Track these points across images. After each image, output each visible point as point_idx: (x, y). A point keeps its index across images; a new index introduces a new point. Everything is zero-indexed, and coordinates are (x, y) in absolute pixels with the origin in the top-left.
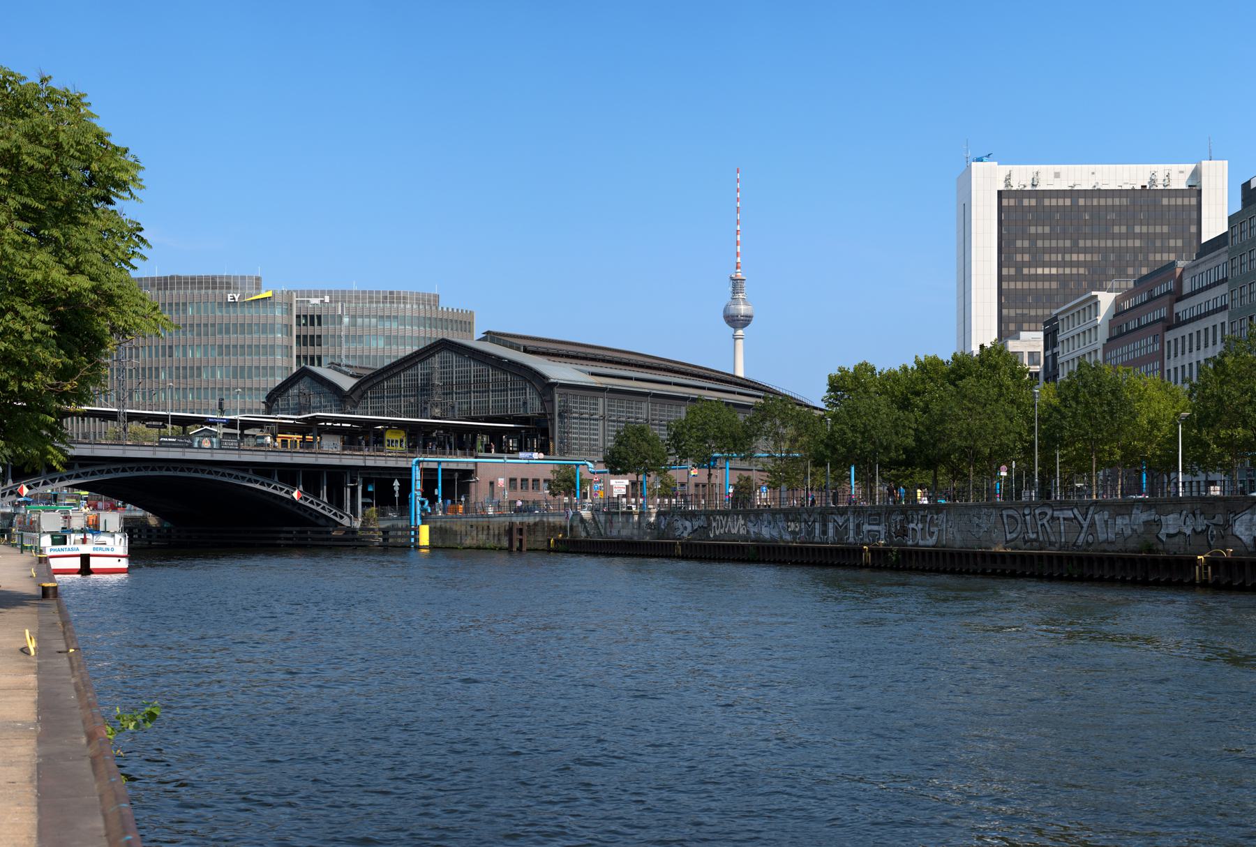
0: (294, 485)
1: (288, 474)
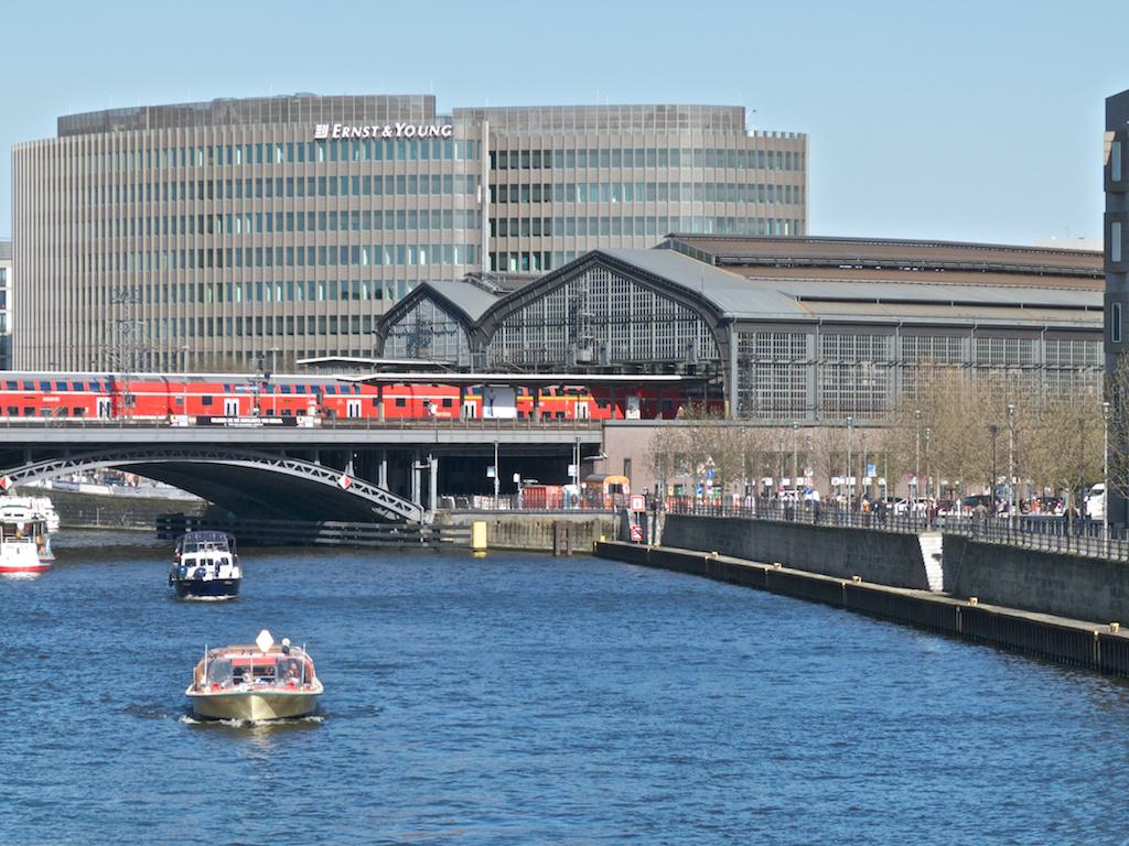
1: (333, 456)
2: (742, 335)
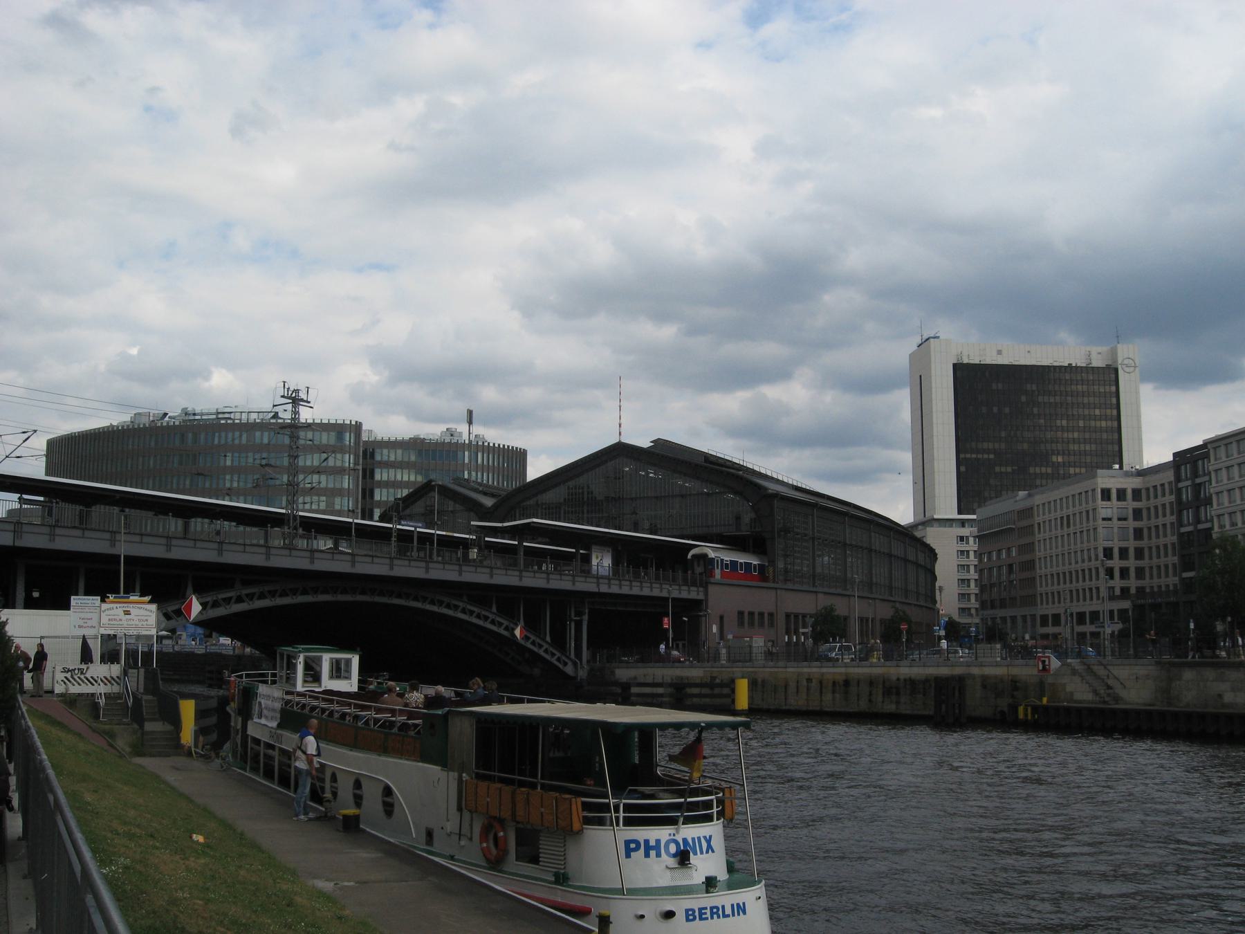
0: (514, 619)
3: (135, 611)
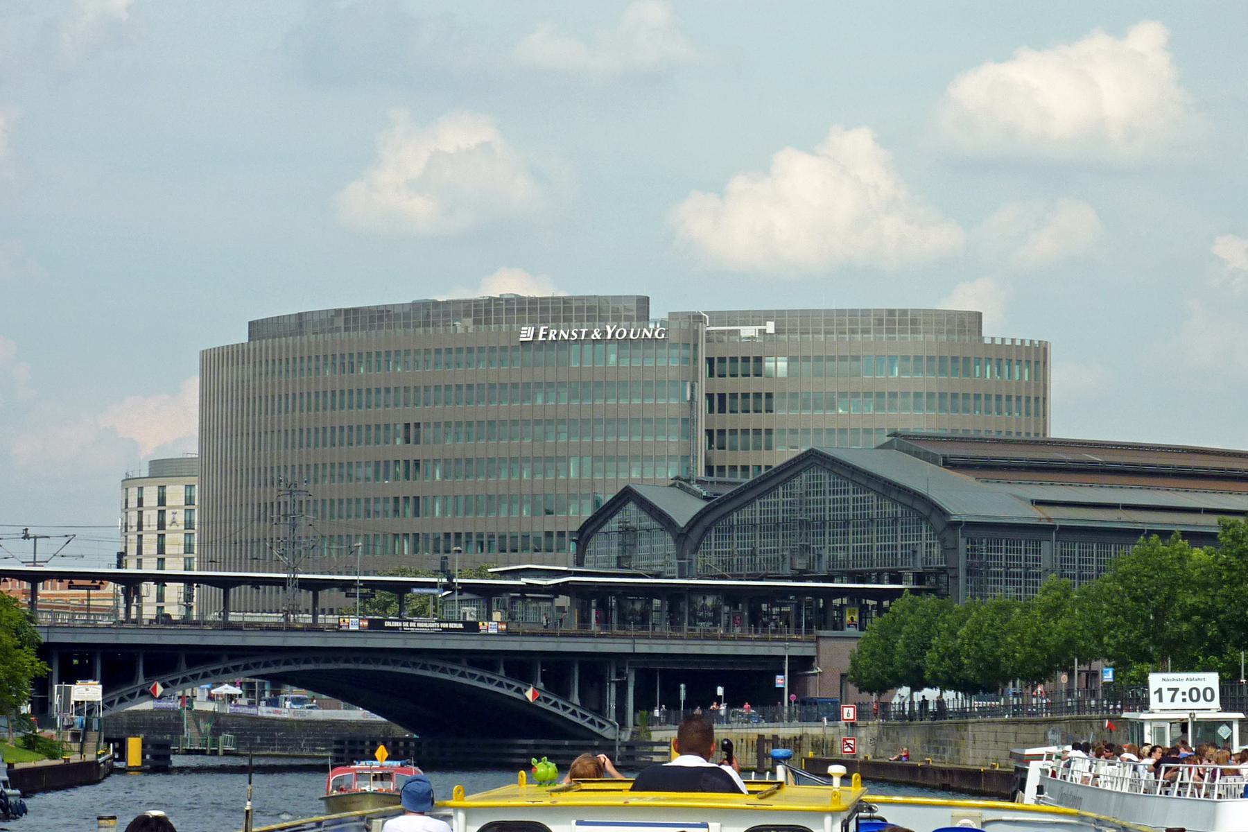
0: (527, 679)
1: (519, 666)
2: (971, 541)
3: (90, 688)
